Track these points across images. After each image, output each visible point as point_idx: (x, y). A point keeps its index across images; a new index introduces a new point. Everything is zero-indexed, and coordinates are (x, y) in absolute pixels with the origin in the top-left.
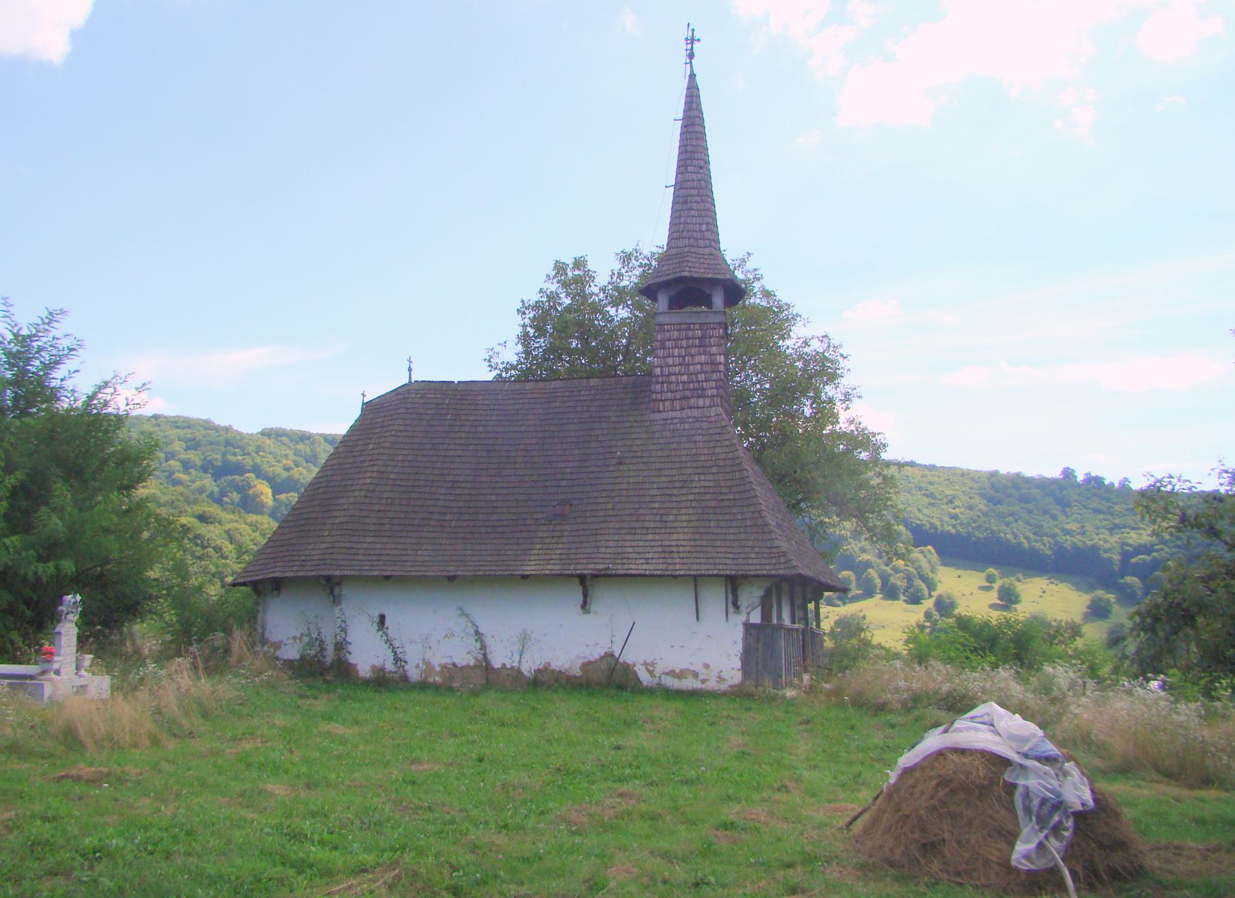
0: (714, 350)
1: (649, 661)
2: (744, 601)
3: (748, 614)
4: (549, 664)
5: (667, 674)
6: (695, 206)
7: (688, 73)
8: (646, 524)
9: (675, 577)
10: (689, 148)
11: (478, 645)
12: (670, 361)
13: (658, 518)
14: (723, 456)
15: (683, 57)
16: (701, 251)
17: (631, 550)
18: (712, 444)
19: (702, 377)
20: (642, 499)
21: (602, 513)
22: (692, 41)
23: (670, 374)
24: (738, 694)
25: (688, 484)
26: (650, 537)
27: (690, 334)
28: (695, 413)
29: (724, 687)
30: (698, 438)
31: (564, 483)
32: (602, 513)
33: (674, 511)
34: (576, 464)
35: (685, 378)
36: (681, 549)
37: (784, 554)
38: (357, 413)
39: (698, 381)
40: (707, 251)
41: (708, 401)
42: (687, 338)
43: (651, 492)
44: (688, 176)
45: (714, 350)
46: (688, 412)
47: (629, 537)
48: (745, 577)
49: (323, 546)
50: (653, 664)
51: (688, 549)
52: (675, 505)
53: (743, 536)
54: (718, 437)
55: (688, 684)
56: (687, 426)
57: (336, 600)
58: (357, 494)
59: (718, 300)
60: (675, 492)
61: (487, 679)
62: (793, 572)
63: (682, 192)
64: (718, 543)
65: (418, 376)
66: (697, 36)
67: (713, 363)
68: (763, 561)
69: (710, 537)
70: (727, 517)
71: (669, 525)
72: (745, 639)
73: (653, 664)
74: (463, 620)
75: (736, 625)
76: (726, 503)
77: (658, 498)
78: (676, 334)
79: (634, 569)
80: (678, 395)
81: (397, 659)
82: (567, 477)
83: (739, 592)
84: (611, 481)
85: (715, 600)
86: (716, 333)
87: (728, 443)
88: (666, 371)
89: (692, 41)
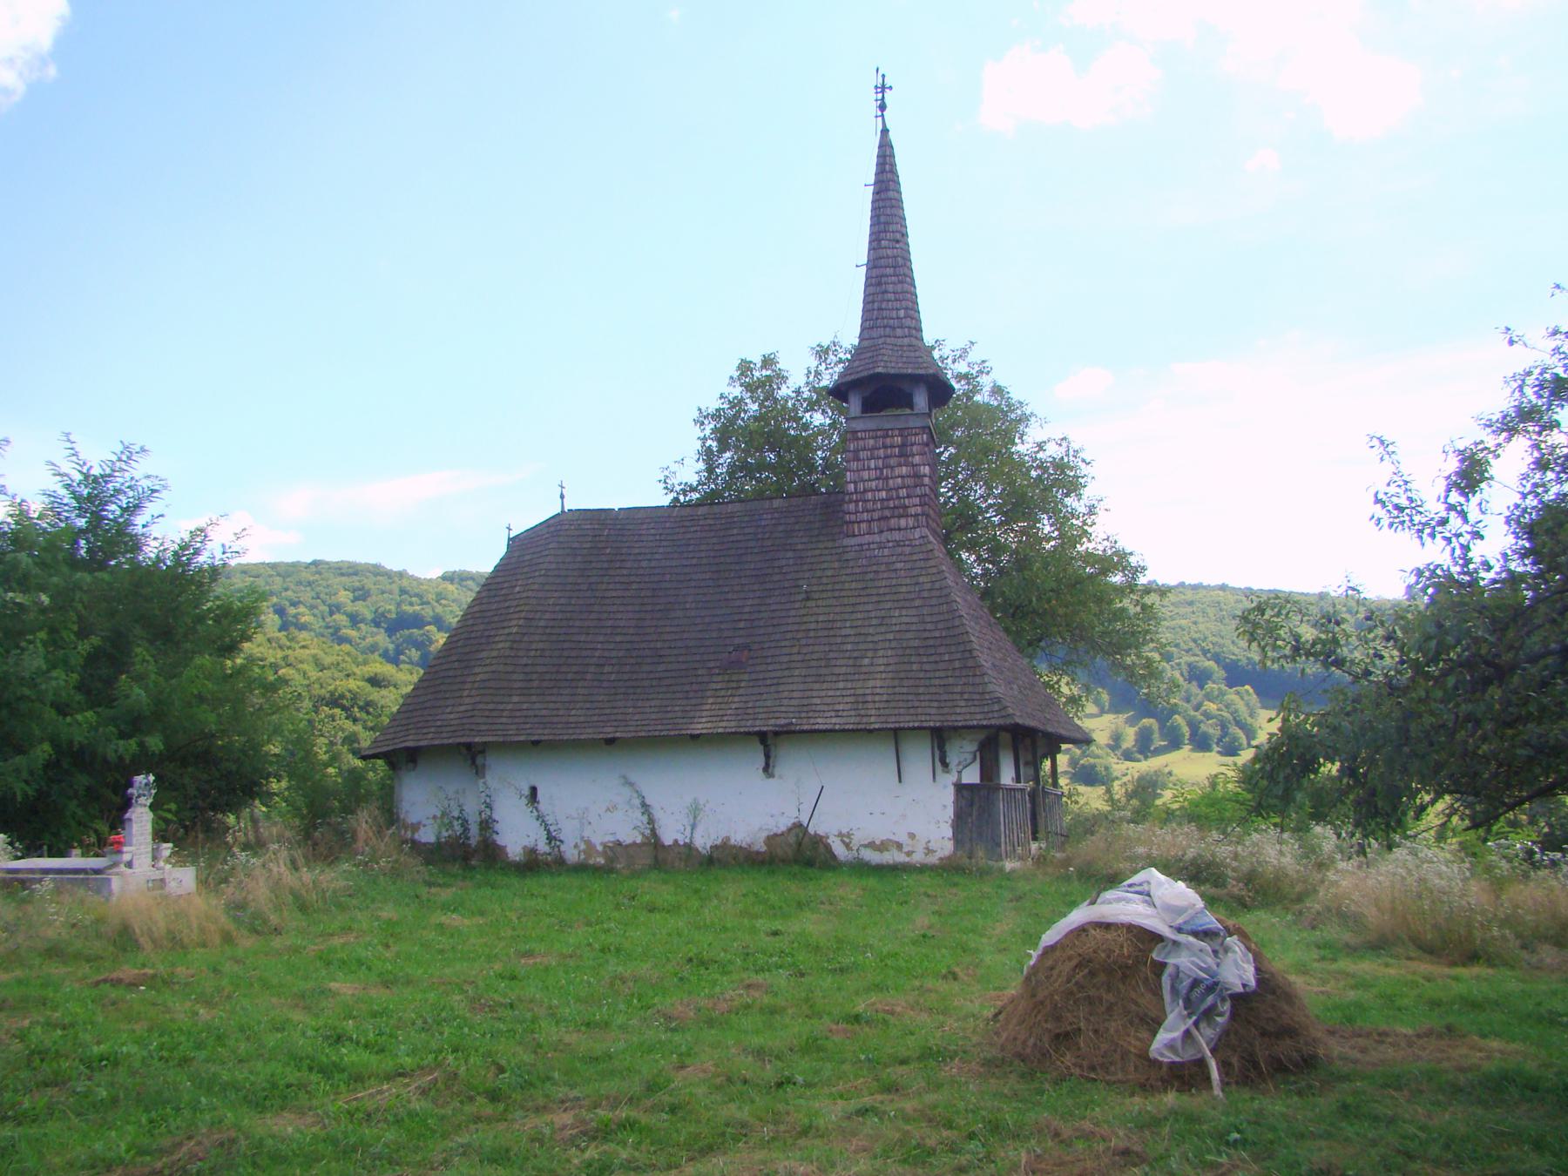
0: (917, 459)
1: (844, 831)
2: (953, 758)
3: (960, 772)
4: (728, 838)
5: (865, 846)
6: (890, 288)
8: (837, 670)
9: (870, 731)
10: (882, 219)
11: (645, 819)
12: (865, 475)
13: (851, 662)
14: (928, 586)
15: (873, 108)
16: (899, 341)
17: (818, 701)
18: (915, 573)
19: (903, 492)
20: (833, 640)
21: (786, 659)
22: (883, 88)
23: (865, 491)
24: (948, 869)
25: (887, 621)
26: (841, 685)
27: (888, 441)
28: (897, 536)
29: (933, 859)
30: (899, 566)
31: (742, 625)
32: (786, 659)
33: (870, 654)
34: (756, 601)
35: (884, 494)
36: (877, 698)
37: (999, 700)
38: (502, 550)
39: (898, 498)
40: (906, 341)
41: (911, 522)
42: (885, 447)
43: (844, 632)
44: (883, 252)
45: (917, 459)
46: (887, 535)
47: (816, 686)
48: (955, 729)
49: (462, 708)
50: (849, 835)
51: (885, 698)
52: (871, 646)
53: (951, 681)
54: (922, 564)
55: (888, 857)
56: (886, 552)
57: (479, 771)
58: (501, 645)
59: (921, 400)
60: (871, 630)
61: (658, 856)
62: (1009, 721)
64: (921, 690)
66: (888, 83)
67: (917, 476)
68: (972, 710)
69: (911, 682)
70: (932, 659)
71: (864, 669)
72: (956, 802)
73: (849, 835)
74: (627, 791)
76: (931, 642)
77: (851, 639)
78: (871, 442)
79: (821, 723)
80: (876, 515)
81: (551, 838)
82: (746, 617)
83: (947, 747)
84: (798, 620)
85: (919, 759)
86: (918, 439)
87: (934, 570)
88: (861, 486)
89: (883, 88)
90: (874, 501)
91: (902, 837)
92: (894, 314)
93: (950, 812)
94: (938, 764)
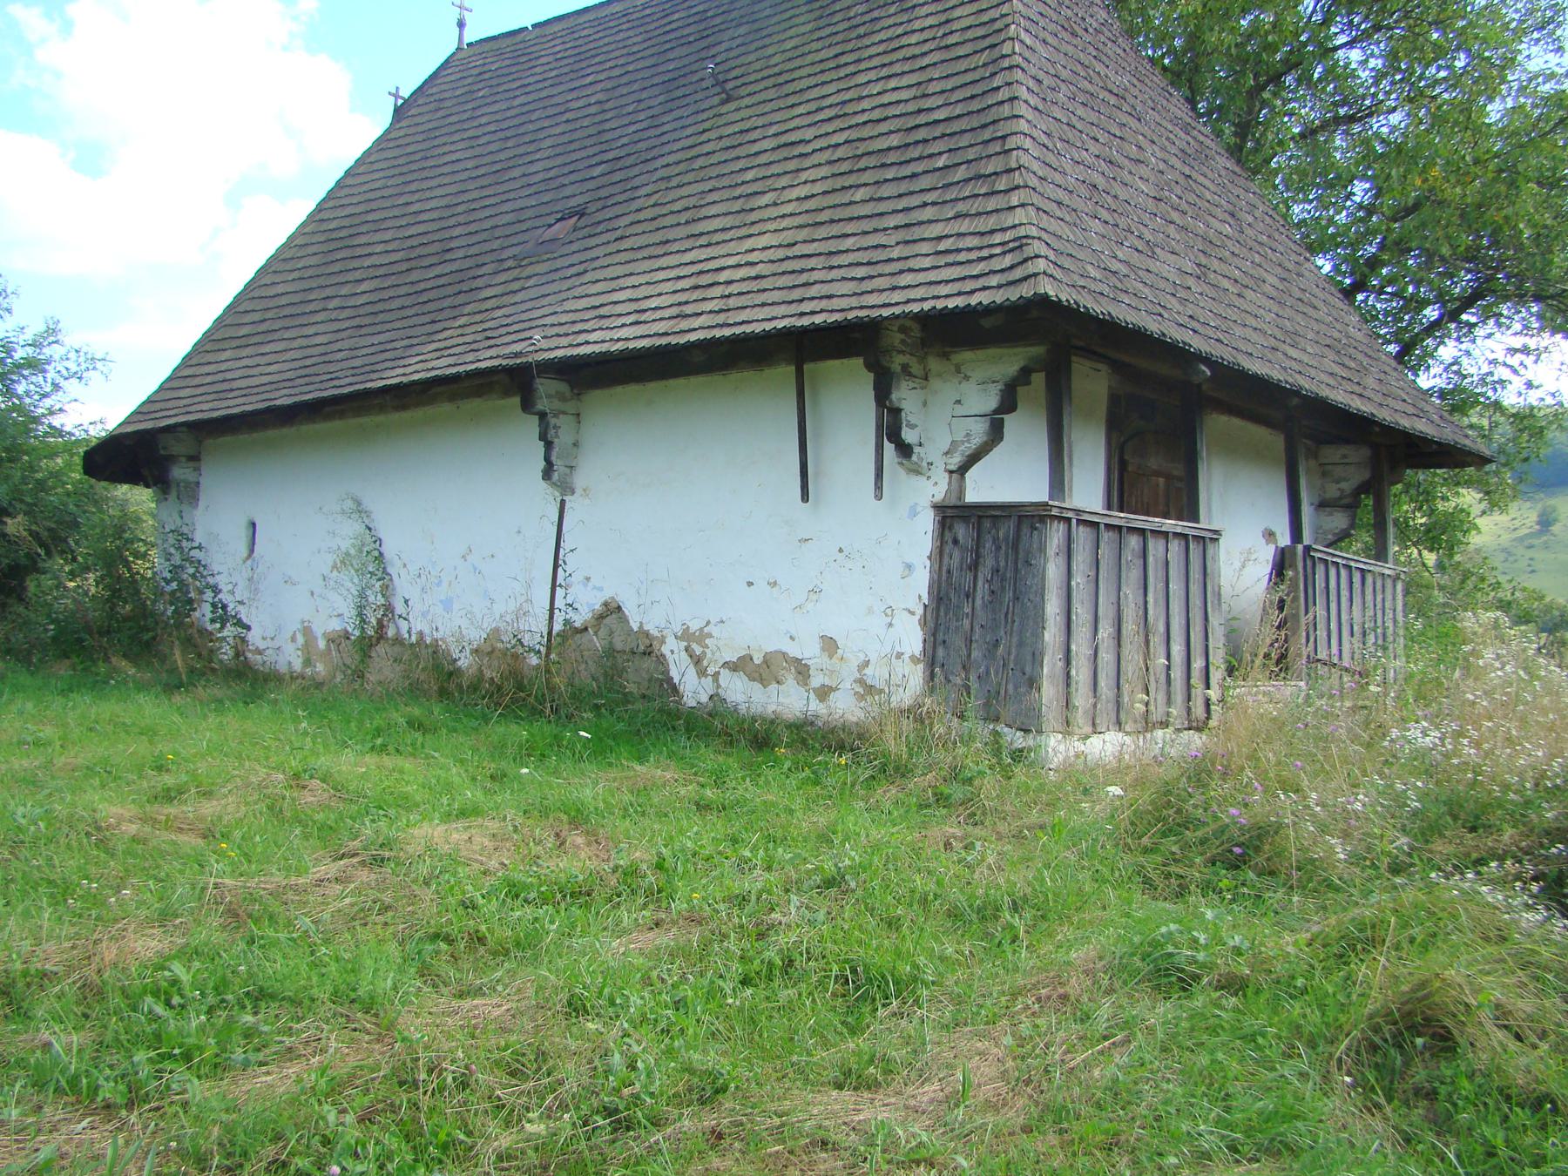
1: (694, 626)
5: (734, 667)
50: (702, 637)
55: (789, 700)
65: (471, 35)
72: (939, 554)
73: (702, 637)
75: (913, 513)
83: (905, 396)
91: (808, 650)
93: (920, 583)
94: (889, 447)
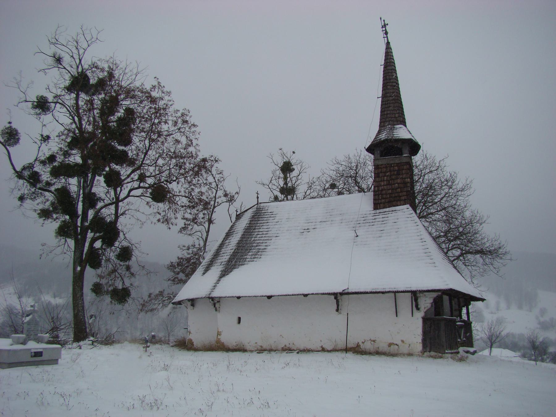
7: (386, 42)
15: (382, 34)
22: (385, 26)
23: (382, 190)
35: (390, 191)
63: (385, 99)
66: (386, 23)
80: (387, 200)
89: (385, 26)
90: (386, 194)
92: (393, 116)
